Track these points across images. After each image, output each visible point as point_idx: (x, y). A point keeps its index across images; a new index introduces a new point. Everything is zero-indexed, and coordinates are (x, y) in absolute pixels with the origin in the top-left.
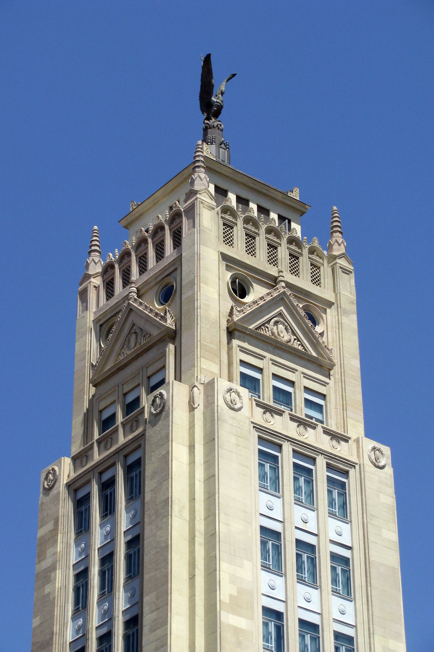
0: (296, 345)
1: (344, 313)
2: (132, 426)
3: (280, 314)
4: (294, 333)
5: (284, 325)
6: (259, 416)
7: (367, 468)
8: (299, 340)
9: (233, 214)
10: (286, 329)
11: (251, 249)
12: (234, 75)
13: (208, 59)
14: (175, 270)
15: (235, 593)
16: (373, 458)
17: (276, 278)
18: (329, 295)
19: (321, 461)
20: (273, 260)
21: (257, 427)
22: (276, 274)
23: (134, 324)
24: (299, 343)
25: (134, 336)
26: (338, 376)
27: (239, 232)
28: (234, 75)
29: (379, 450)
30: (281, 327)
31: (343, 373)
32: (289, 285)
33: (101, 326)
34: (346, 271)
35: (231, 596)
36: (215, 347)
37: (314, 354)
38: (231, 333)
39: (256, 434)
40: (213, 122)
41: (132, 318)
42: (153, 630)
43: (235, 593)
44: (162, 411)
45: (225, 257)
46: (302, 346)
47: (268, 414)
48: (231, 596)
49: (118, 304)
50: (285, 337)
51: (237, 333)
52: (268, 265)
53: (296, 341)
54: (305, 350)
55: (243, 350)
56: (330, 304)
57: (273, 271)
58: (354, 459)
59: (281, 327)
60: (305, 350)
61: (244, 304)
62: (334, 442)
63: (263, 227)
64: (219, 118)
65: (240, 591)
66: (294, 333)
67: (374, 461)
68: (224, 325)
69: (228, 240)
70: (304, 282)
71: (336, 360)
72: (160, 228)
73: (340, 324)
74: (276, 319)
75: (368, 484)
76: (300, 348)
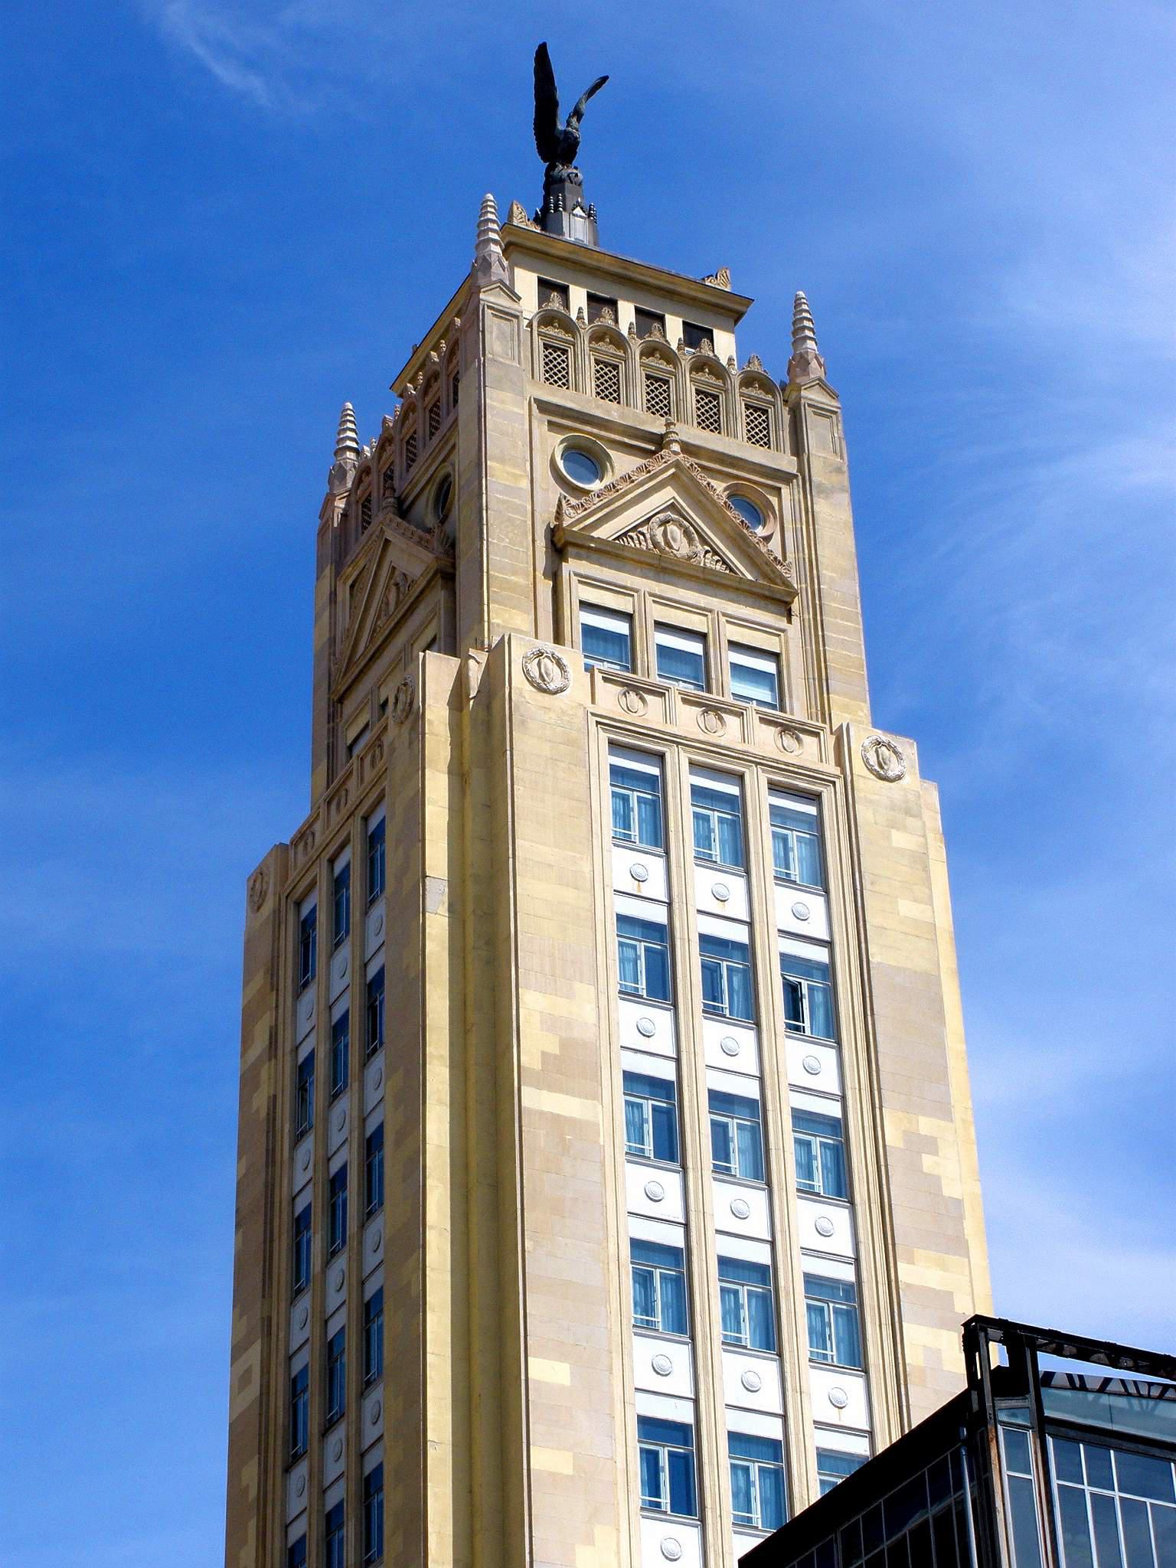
0: (710, 562)
1: (819, 492)
2: (373, 756)
3: (673, 507)
4: (704, 541)
5: (681, 526)
6: (610, 700)
8: (716, 553)
9: (669, 357)
10: (687, 533)
11: (610, 388)
13: (604, 79)
14: (454, 447)
15: (554, 1049)
16: (873, 760)
17: (662, 437)
18: (787, 462)
19: (757, 782)
20: (659, 404)
21: (605, 723)
22: (663, 430)
23: (394, 568)
24: (716, 558)
25: (394, 589)
27: (585, 361)
29: (889, 746)
31: (818, 610)
32: (688, 449)
33: (352, 586)
34: (821, 411)
36: (525, 581)
37: (750, 577)
39: (604, 736)
40: (562, 171)
41: (392, 556)
45: (544, 407)
46: (724, 562)
47: (632, 695)
50: (681, 547)
51: (571, 550)
52: (698, 431)
53: (709, 555)
54: (731, 570)
55: (587, 581)
56: (787, 478)
57: (657, 426)
60: (731, 570)
61: (587, 492)
62: (788, 740)
63: (686, 363)
64: (575, 163)
65: (565, 1044)
66: (704, 541)
67: (877, 768)
69: (557, 373)
70: (736, 444)
74: (661, 516)
75: (863, 813)
76: (719, 567)
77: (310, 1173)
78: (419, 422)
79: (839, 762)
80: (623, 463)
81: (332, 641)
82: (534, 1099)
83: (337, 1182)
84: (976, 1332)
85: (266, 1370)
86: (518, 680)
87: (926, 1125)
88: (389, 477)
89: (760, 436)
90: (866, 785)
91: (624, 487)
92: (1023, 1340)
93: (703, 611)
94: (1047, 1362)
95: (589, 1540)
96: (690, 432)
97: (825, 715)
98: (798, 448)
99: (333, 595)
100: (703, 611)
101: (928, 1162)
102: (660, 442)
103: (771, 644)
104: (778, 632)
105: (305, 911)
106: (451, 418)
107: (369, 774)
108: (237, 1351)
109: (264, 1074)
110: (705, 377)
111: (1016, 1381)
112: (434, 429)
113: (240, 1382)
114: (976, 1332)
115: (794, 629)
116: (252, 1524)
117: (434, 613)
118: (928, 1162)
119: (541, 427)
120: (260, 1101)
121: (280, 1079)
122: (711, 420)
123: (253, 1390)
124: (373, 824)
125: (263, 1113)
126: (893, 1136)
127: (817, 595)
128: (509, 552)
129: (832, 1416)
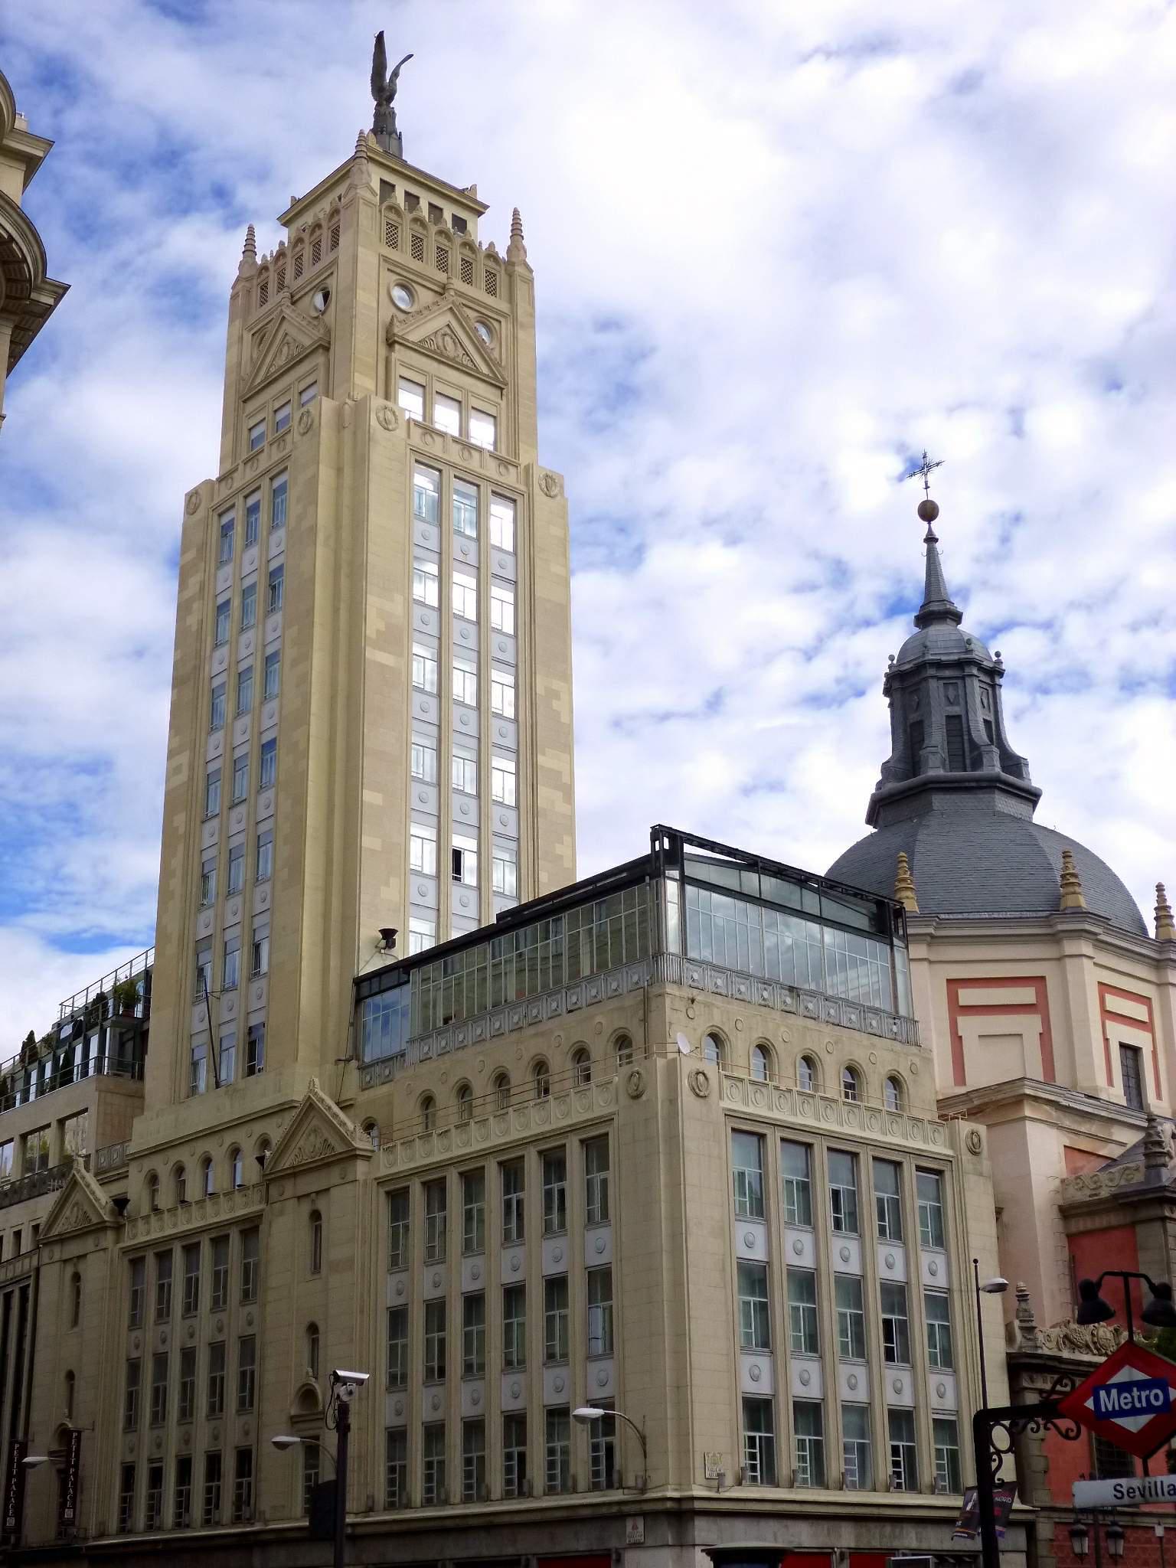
0: (465, 361)
7: (536, 498)
11: (418, 253)
15: (382, 627)
18: (504, 306)
26: (511, 397)
30: (447, 338)
31: (516, 394)
35: (378, 631)
36: (372, 361)
38: (391, 343)
41: (285, 326)
42: (295, 663)
43: (382, 627)
44: (310, 429)
45: (386, 259)
48: (378, 631)
49: (270, 312)
50: (451, 349)
55: (404, 365)
57: (441, 277)
58: (522, 488)
59: (447, 338)
68: (382, 335)
70: (478, 292)
71: (509, 380)
72: (318, 226)
73: (515, 337)
76: (470, 364)
77: (225, 666)
78: (308, 252)
79: (527, 485)
80: (425, 296)
81: (240, 364)
82: (373, 655)
83: (242, 676)
84: (658, 832)
85: (192, 768)
86: (374, 422)
87: (557, 685)
88: (281, 275)
89: (492, 290)
90: (539, 497)
91: (426, 312)
92: (678, 838)
93: (459, 388)
94: (688, 849)
95: (387, 884)
96: (458, 284)
97: (516, 455)
98: (511, 300)
99: (241, 338)
100: (459, 388)
101: (555, 704)
102: (444, 287)
103: (493, 411)
104: (496, 405)
105: (225, 519)
106: (331, 257)
107: (276, 456)
108: (172, 754)
109: (196, 606)
110: (467, 252)
111: (674, 857)
112: (317, 258)
113: (172, 772)
114: (658, 832)
115: (503, 403)
116: (181, 848)
117: (314, 370)
118: (555, 704)
119: (385, 274)
120: (192, 621)
121: (202, 611)
122: (468, 278)
123: (183, 777)
124: (276, 483)
125: (194, 628)
126: (540, 689)
127: (516, 385)
128: (365, 342)
129: (501, 830)
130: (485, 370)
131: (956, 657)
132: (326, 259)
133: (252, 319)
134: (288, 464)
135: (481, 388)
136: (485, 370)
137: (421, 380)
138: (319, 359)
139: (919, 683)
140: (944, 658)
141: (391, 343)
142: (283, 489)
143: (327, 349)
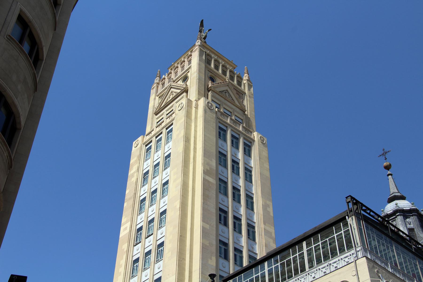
12: (211, 30)
15: (209, 169)
28: (211, 30)
95: (211, 259)
107: (168, 120)
130: (238, 104)
131: (409, 208)
132: (186, 68)
133: (159, 92)
134: (174, 122)
135: (238, 110)
136: (238, 104)
137: (219, 103)
138: (185, 94)
139: (396, 217)
140: (404, 208)
141: (209, 91)
142: (171, 131)
143: (187, 92)
